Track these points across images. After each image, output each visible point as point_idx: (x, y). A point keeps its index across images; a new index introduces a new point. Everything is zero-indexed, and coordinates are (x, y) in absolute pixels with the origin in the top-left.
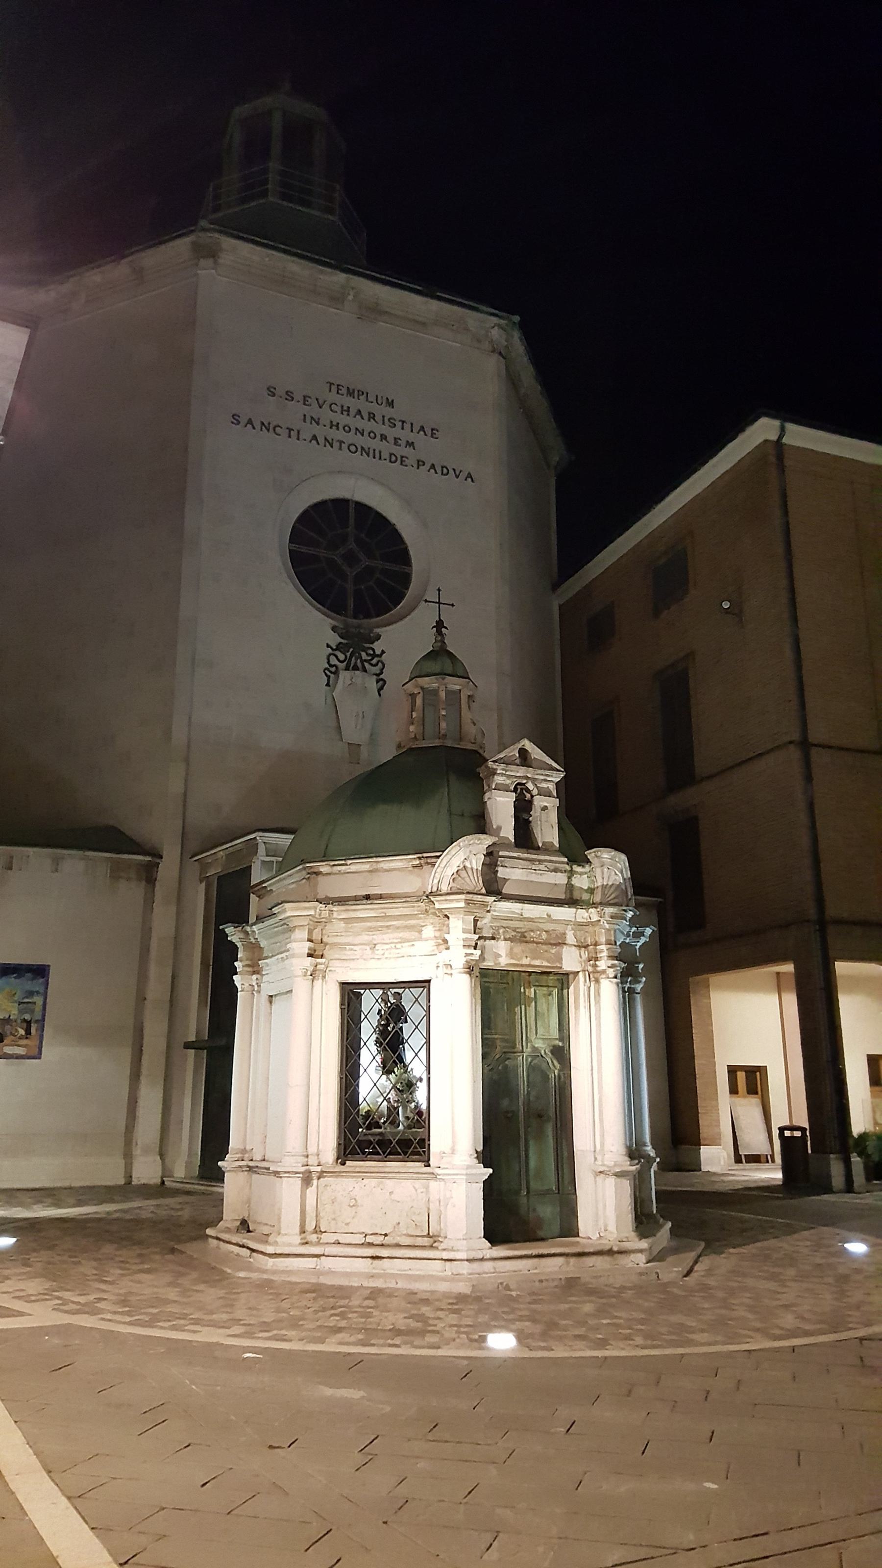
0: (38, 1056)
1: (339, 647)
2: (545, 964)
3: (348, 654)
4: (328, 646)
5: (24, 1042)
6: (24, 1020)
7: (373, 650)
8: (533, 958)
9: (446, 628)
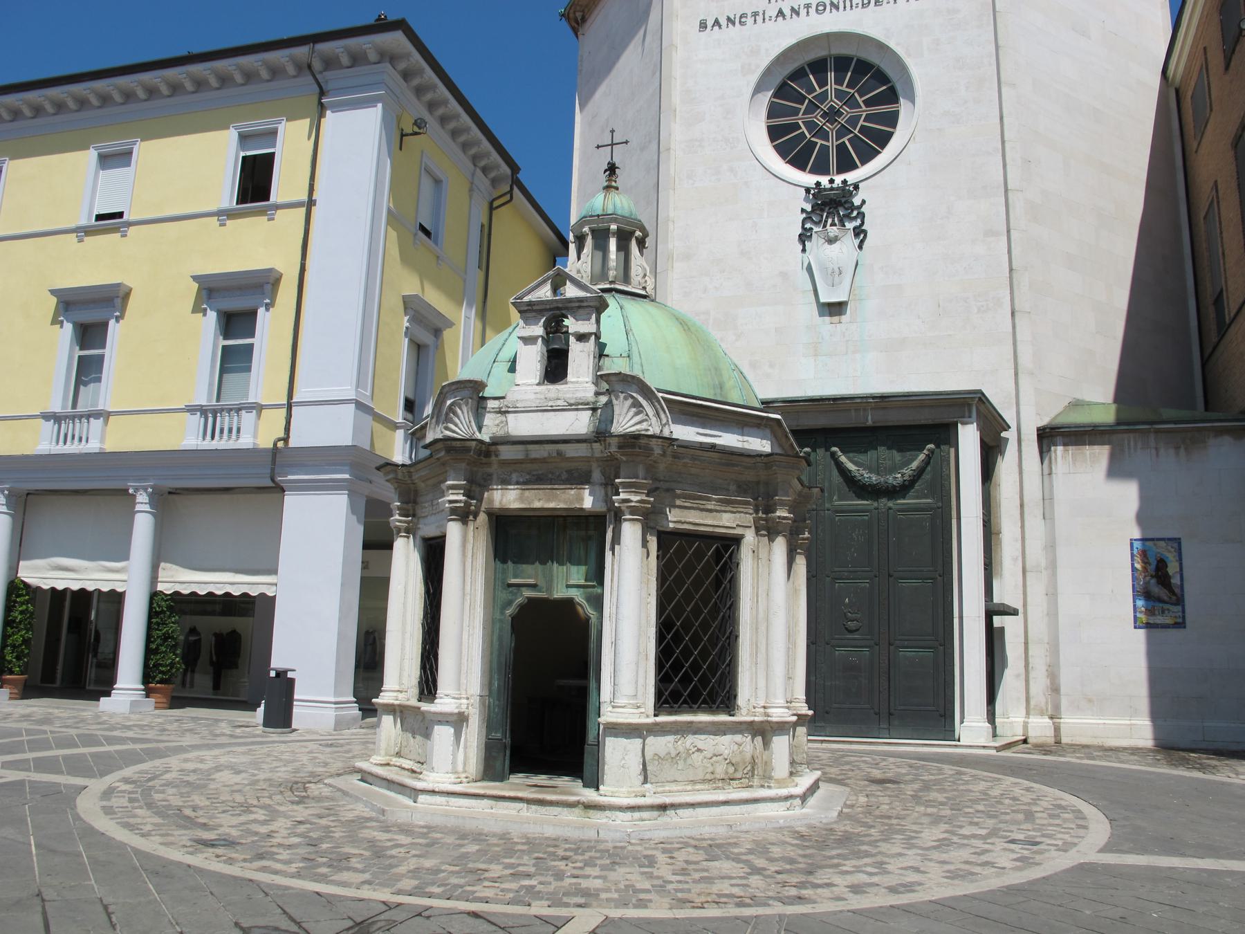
2: (562, 506)
8: (549, 500)
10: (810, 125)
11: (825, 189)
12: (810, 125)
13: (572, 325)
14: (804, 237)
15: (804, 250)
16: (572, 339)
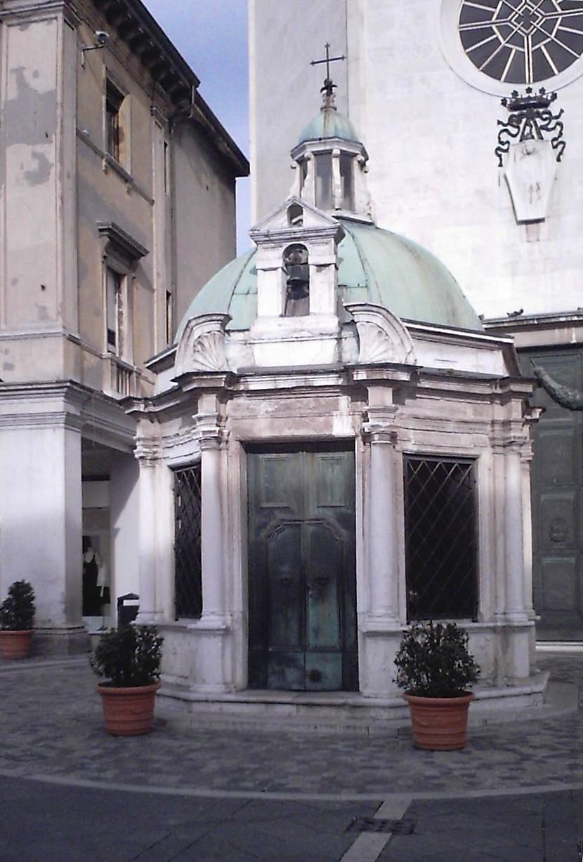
1: (513, 121)
3: (522, 126)
7: (549, 113)
8: (297, 428)
11: (522, 99)
12: (505, 30)
15: (501, 165)
16: (312, 269)
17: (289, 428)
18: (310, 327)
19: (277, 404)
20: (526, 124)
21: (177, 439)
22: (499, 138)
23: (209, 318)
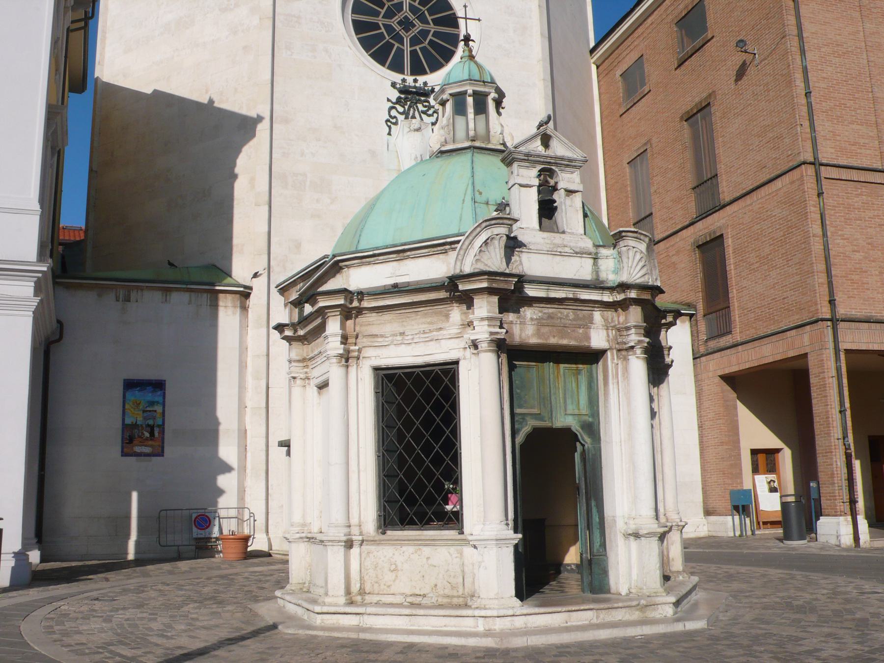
0: (161, 454)
1: (399, 101)
2: (573, 343)
3: (406, 107)
4: (388, 100)
5: (150, 443)
6: (148, 425)
7: (428, 102)
9: (473, 41)
10: (389, 28)
11: (410, 87)
13: (566, 179)
14: (391, 122)
15: (389, 134)
17: (554, 337)
18: (572, 244)
19: (541, 312)
20: (410, 107)
21: (399, 338)
22: (389, 112)
23: (501, 221)
